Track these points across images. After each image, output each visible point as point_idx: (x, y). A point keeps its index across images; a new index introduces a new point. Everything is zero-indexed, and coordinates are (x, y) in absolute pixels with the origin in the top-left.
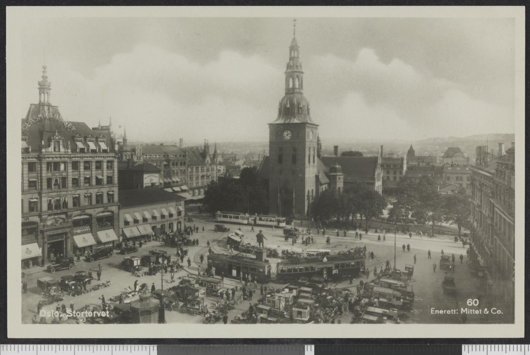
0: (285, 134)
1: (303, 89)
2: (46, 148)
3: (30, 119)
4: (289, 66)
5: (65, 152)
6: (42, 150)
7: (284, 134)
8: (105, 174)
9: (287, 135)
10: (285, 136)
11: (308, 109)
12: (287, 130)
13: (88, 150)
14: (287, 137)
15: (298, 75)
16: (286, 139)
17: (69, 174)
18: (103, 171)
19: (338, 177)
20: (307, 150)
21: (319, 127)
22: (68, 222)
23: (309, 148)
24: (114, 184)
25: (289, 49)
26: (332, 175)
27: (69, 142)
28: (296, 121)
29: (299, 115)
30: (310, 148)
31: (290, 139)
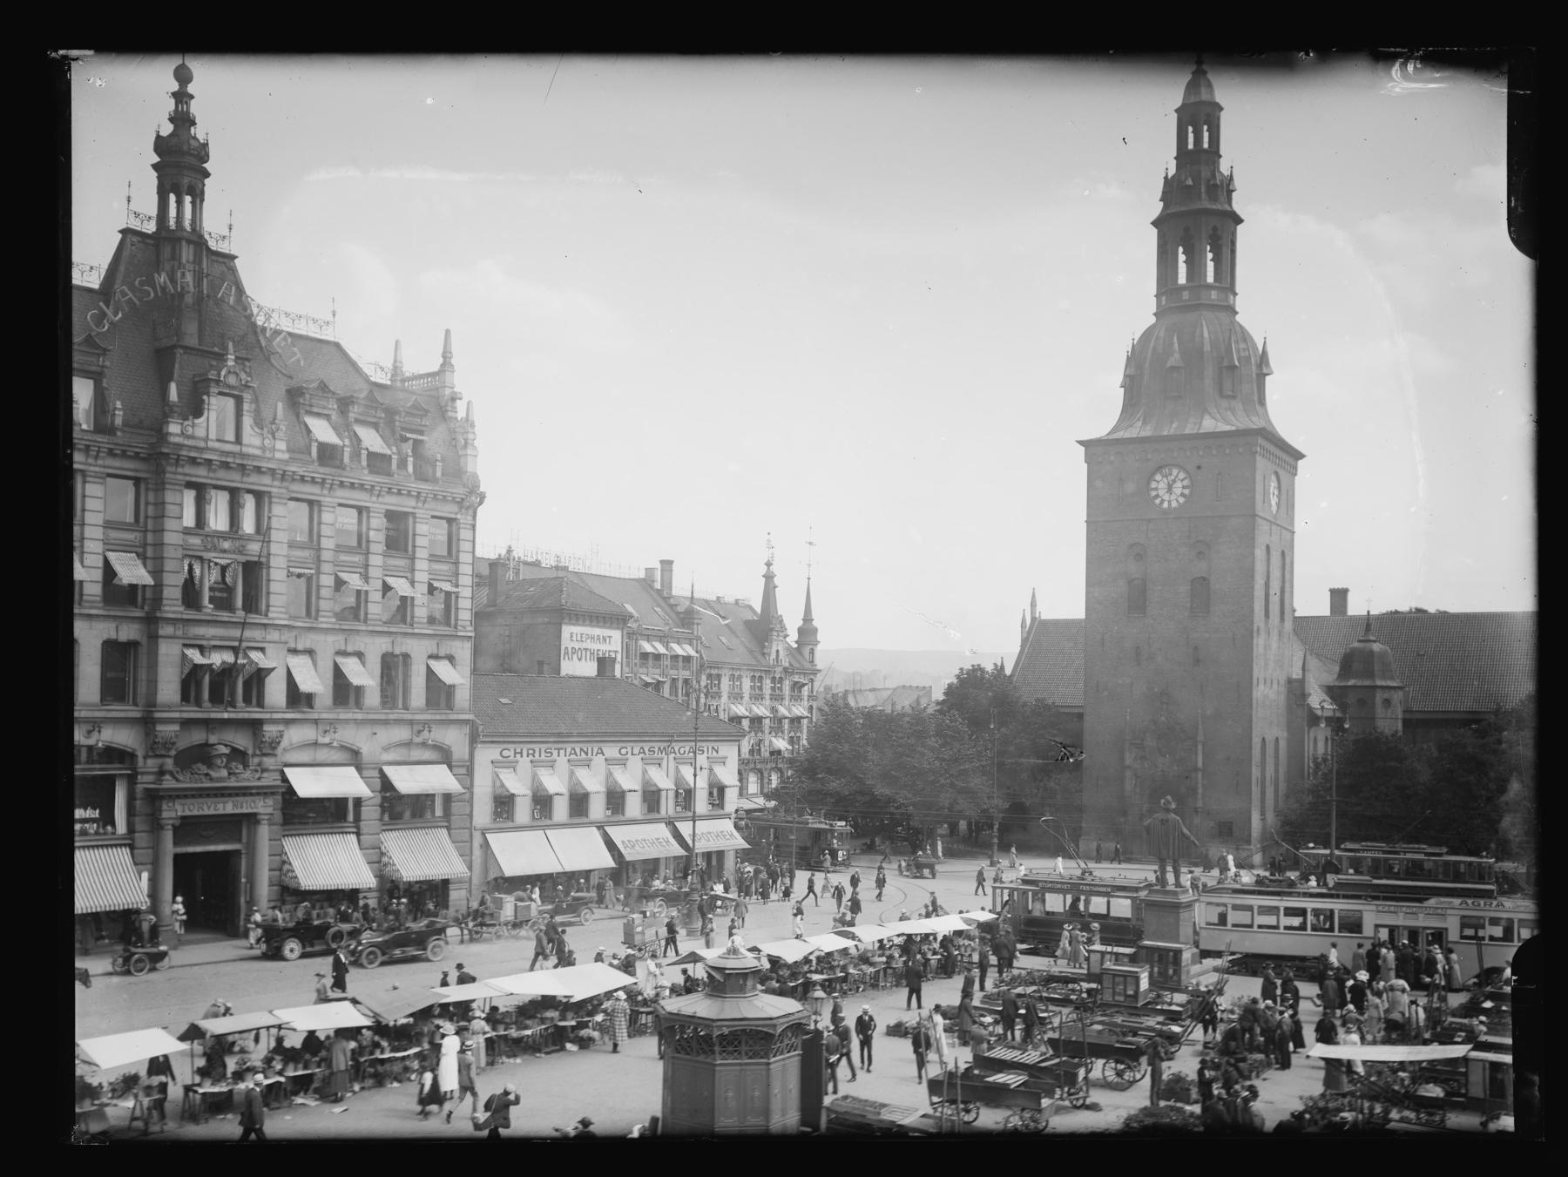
0: (1160, 483)
1: (1235, 294)
2: (186, 419)
3: (119, 287)
5: (263, 448)
6: (168, 423)
7: (1153, 485)
8: (422, 577)
9: (1170, 489)
10: (1161, 493)
11: (1261, 377)
13: (356, 455)
14: (1166, 497)
15: (1215, 229)
16: (1165, 505)
17: (274, 548)
18: (413, 558)
20: (1260, 553)
22: (263, 771)
23: (1264, 548)
24: (456, 627)
27: (280, 405)
28: (1209, 425)
29: (1224, 403)
30: (1268, 547)
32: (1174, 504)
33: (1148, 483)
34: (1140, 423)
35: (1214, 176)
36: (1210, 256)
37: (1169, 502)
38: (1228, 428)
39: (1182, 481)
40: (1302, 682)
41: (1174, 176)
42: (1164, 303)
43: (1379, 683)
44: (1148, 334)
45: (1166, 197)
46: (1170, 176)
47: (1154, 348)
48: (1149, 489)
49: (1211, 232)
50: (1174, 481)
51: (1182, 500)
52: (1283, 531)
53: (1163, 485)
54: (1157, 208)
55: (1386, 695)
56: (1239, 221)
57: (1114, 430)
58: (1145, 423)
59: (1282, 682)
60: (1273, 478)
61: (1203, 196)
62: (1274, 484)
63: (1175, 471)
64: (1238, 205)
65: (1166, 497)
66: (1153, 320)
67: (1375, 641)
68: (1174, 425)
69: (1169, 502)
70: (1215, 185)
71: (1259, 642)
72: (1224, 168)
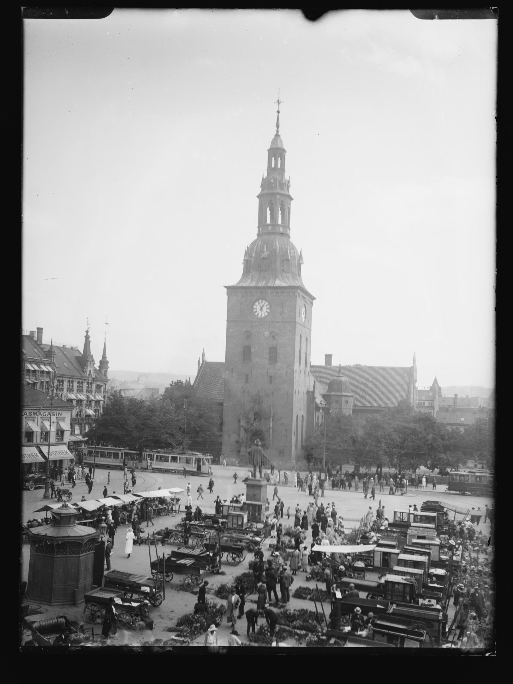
0: (257, 306)
4: (266, 184)
7: (255, 307)
9: (261, 309)
11: (299, 265)
12: (263, 299)
14: (260, 312)
15: (282, 201)
16: (260, 316)
19: (344, 399)
20: (297, 338)
21: (314, 301)
23: (299, 336)
25: (266, 154)
26: (334, 395)
28: (278, 283)
29: (284, 274)
30: (301, 336)
31: (266, 317)
32: (263, 316)
33: (253, 306)
34: (250, 280)
35: (282, 179)
36: (280, 212)
37: (261, 315)
38: (285, 285)
39: (267, 306)
40: (313, 392)
41: (266, 178)
42: (261, 230)
43: (344, 394)
44: (253, 244)
45: (262, 186)
46: (264, 178)
47: (256, 250)
48: (253, 309)
49: (280, 203)
50: (263, 306)
51: (266, 314)
52: (307, 329)
53: (258, 308)
54: (259, 190)
55: (346, 399)
56: (291, 199)
57: (237, 284)
58: (252, 280)
59: (305, 392)
60: (304, 307)
61: (278, 187)
62: (304, 309)
63: (264, 302)
64: (292, 192)
65: (260, 312)
66: (256, 237)
67: (342, 377)
68: (264, 282)
69: (261, 315)
70: (283, 184)
71: (296, 375)
72: (286, 176)
